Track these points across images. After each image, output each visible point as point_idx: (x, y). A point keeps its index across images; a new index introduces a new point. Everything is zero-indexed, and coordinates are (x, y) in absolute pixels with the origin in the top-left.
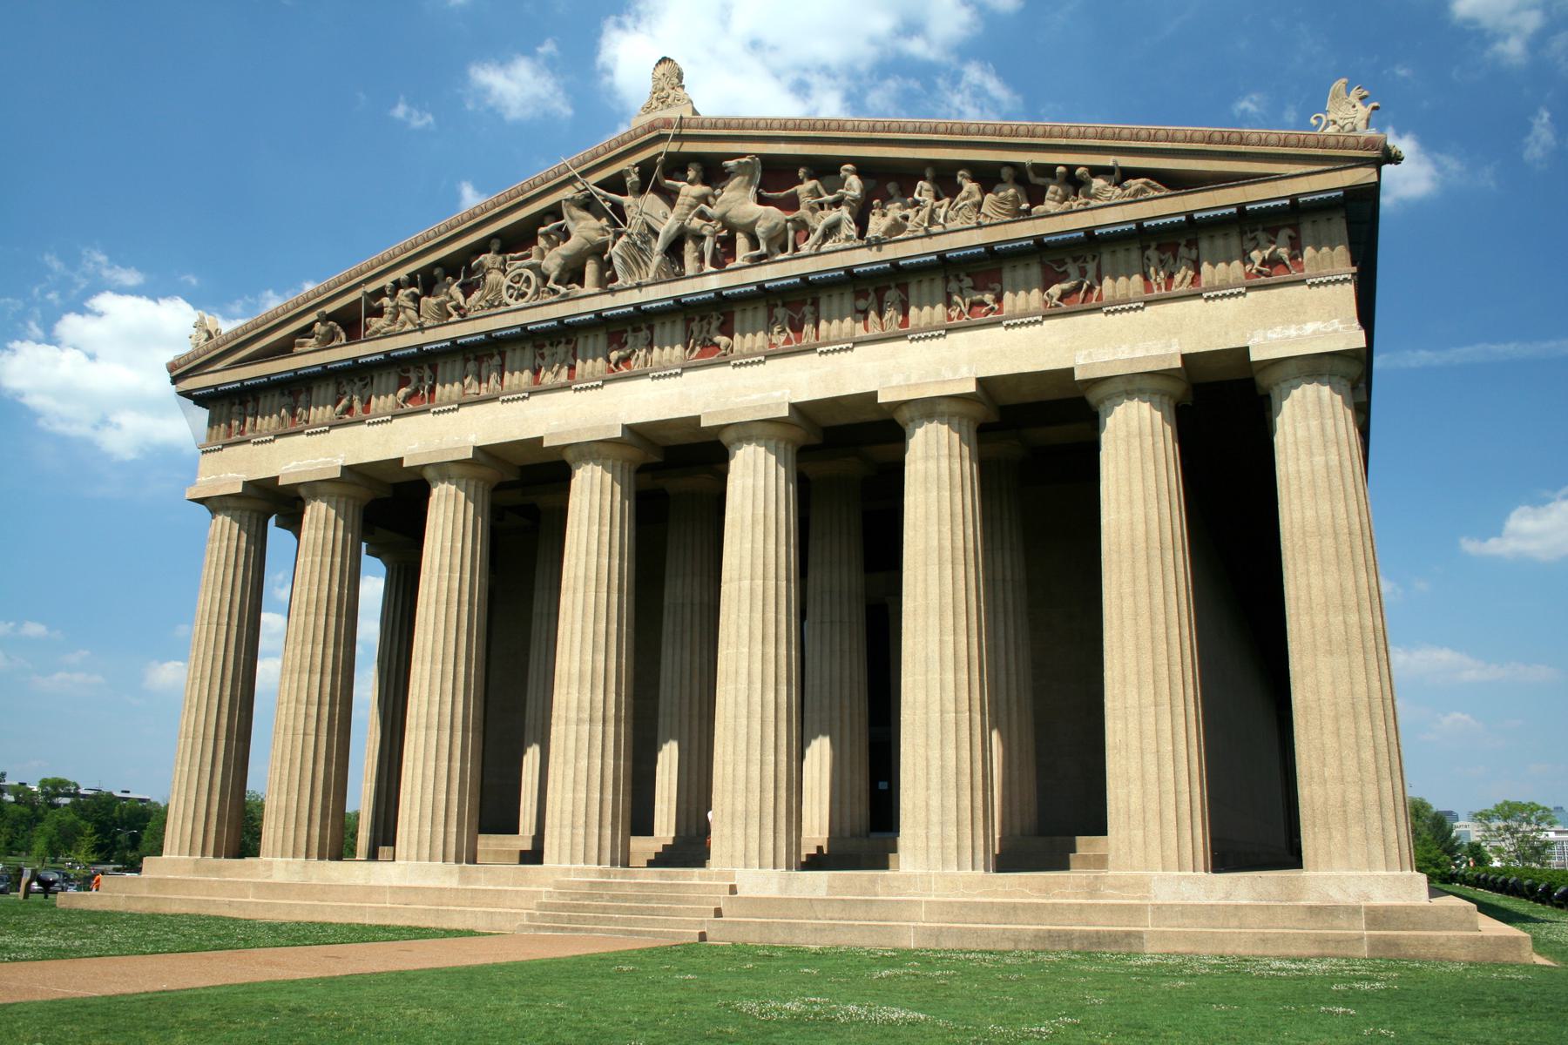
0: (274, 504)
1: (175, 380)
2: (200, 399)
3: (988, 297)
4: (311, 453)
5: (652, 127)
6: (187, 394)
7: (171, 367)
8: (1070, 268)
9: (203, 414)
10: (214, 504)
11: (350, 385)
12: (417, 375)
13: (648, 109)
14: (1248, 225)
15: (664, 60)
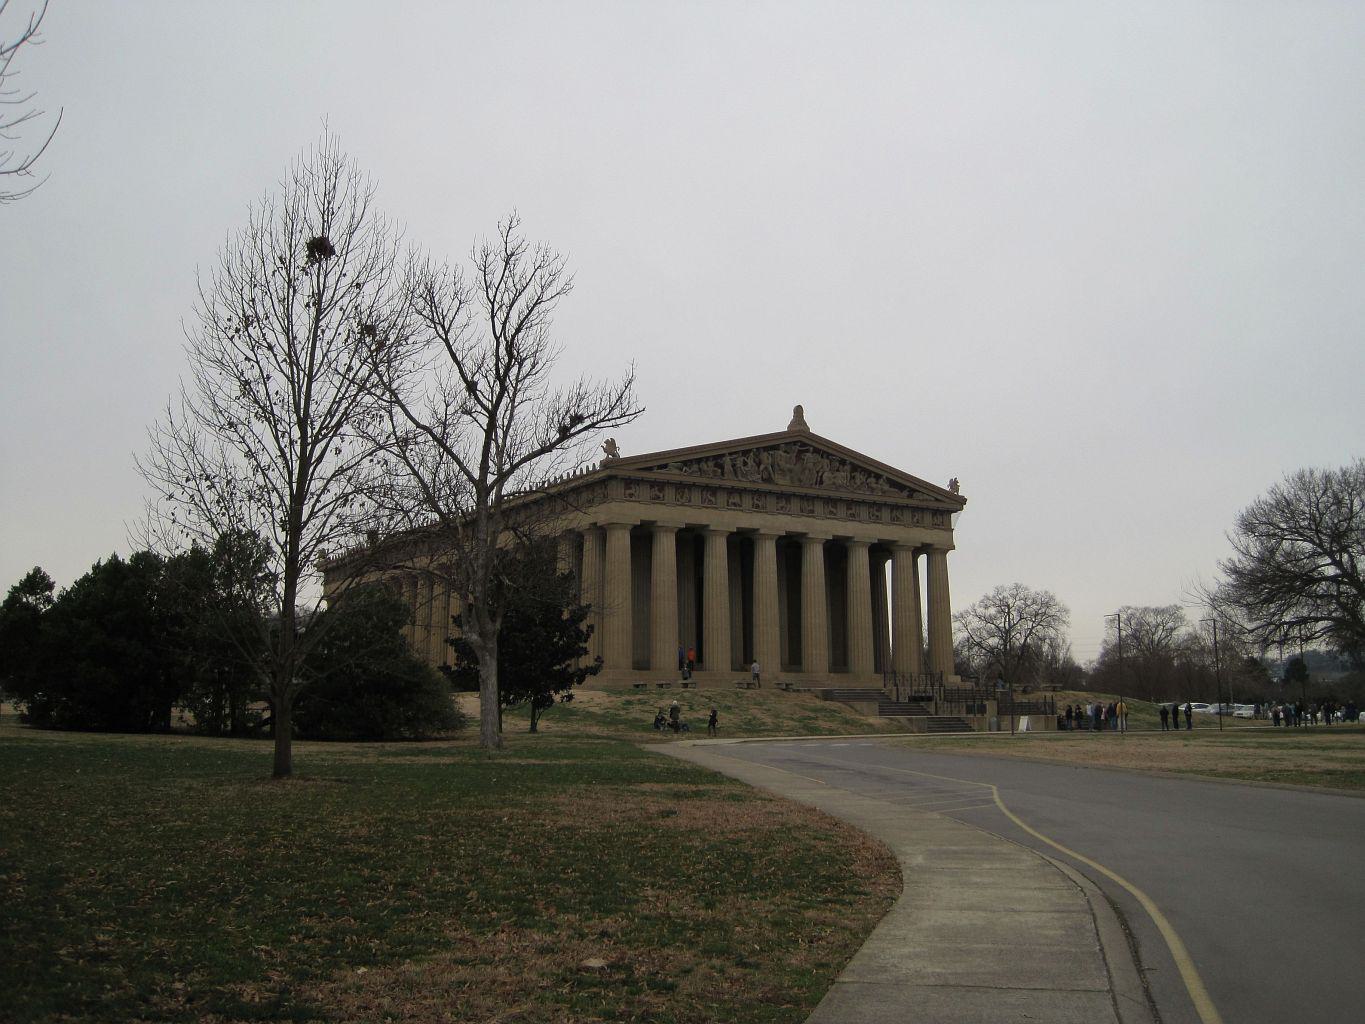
3: (877, 514)
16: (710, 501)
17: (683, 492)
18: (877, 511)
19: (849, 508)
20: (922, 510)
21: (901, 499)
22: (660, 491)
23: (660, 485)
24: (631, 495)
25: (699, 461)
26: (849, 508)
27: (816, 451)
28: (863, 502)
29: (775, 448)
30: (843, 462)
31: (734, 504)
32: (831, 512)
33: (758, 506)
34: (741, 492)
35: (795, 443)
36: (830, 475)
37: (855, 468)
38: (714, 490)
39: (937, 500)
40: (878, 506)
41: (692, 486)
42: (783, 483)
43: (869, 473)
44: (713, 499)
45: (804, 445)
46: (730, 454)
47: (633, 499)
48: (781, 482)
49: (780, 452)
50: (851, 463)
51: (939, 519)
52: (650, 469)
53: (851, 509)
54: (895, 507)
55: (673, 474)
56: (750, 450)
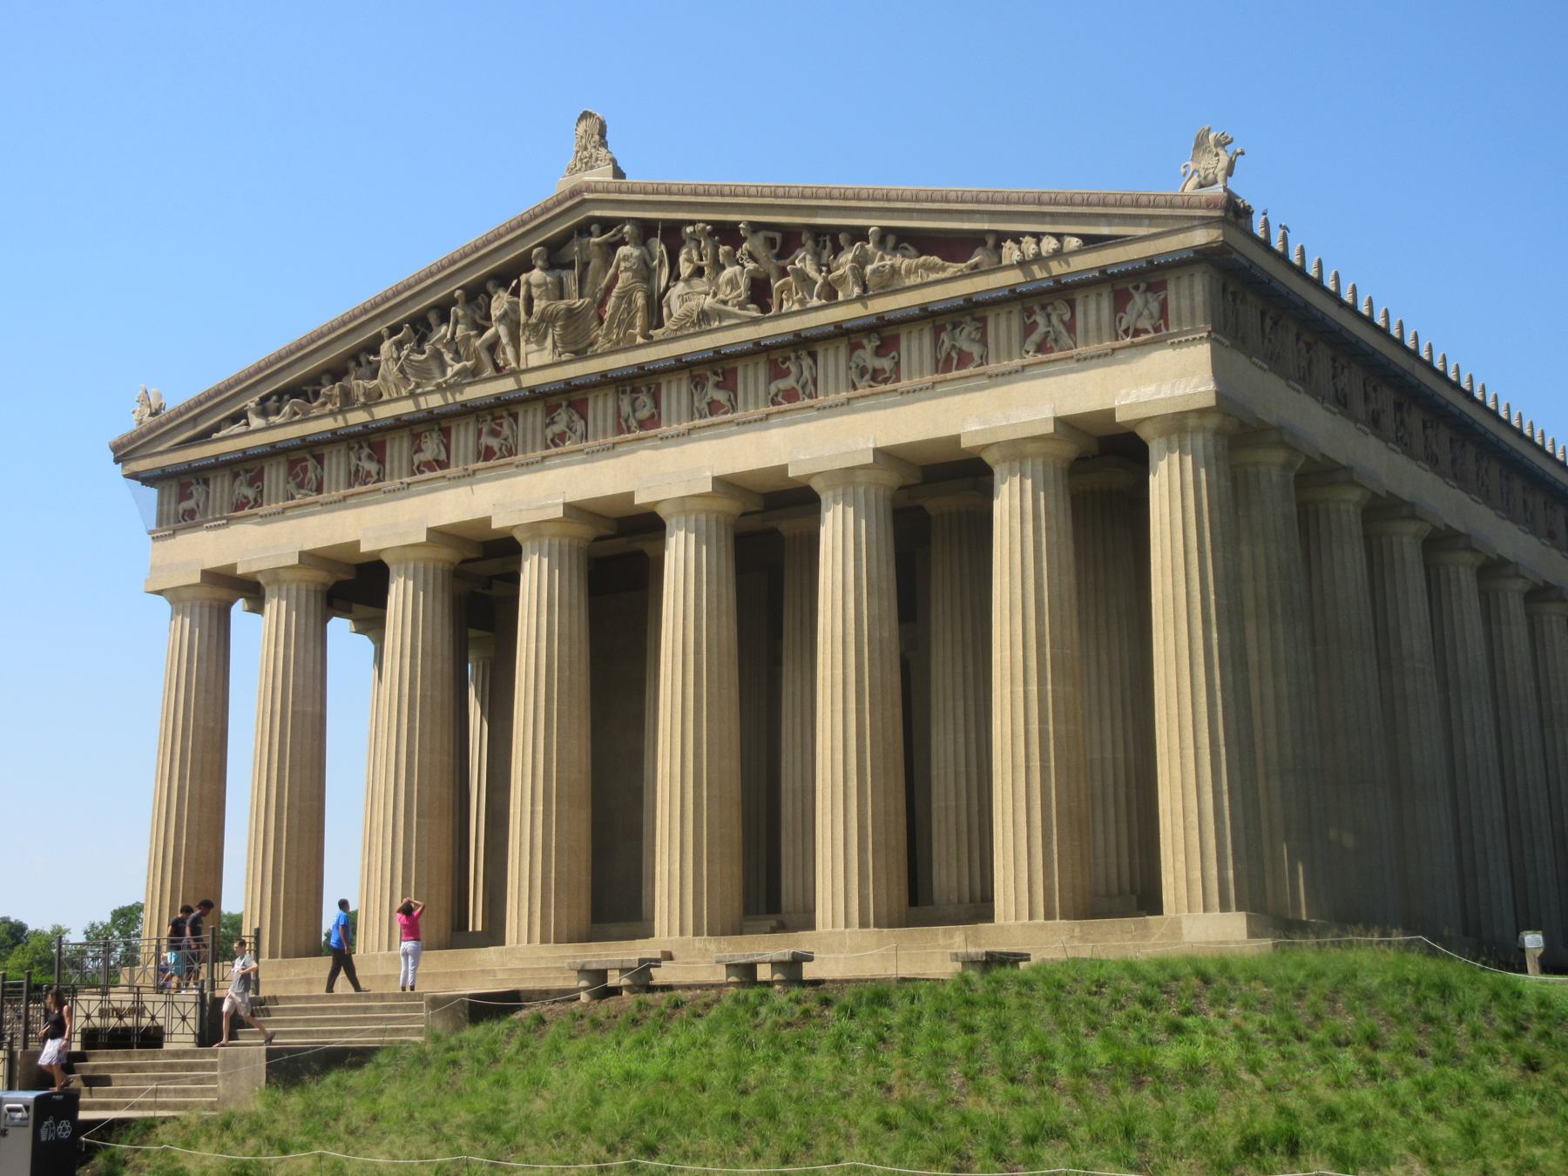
0: (233, 587)
1: (117, 461)
2: (147, 479)
3: (885, 364)
4: (266, 541)
5: (574, 193)
6: (134, 476)
7: (116, 448)
8: (956, 337)
9: (152, 494)
10: (175, 596)
11: (302, 468)
12: (371, 454)
13: (572, 171)
14: (1121, 285)
15: (585, 115)
16: (369, 474)
17: (305, 470)
18: (879, 352)
19: (777, 373)
20: (1064, 292)
21: (948, 285)
22: (251, 484)
23: (248, 466)
24: (190, 514)
25: (336, 372)
26: (777, 373)
27: (646, 230)
28: (804, 344)
29: (525, 264)
30: (727, 234)
31: (429, 466)
32: (714, 407)
33: (488, 454)
34: (438, 423)
35: (583, 229)
36: (700, 285)
37: (785, 241)
38: (372, 440)
39: (1091, 242)
40: (885, 332)
41: (313, 448)
42: (541, 363)
43: (828, 240)
44: (372, 467)
45: (607, 224)
46: (394, 330)
47: (198, 518)
48: (534, 360)
49: (536, 275)
50: (755, 227)
51: (1141, 305)
52: (204, 437)
53: (787, 373)
54: (931, 318)
55: (258, 434)
56: (451, 301)
